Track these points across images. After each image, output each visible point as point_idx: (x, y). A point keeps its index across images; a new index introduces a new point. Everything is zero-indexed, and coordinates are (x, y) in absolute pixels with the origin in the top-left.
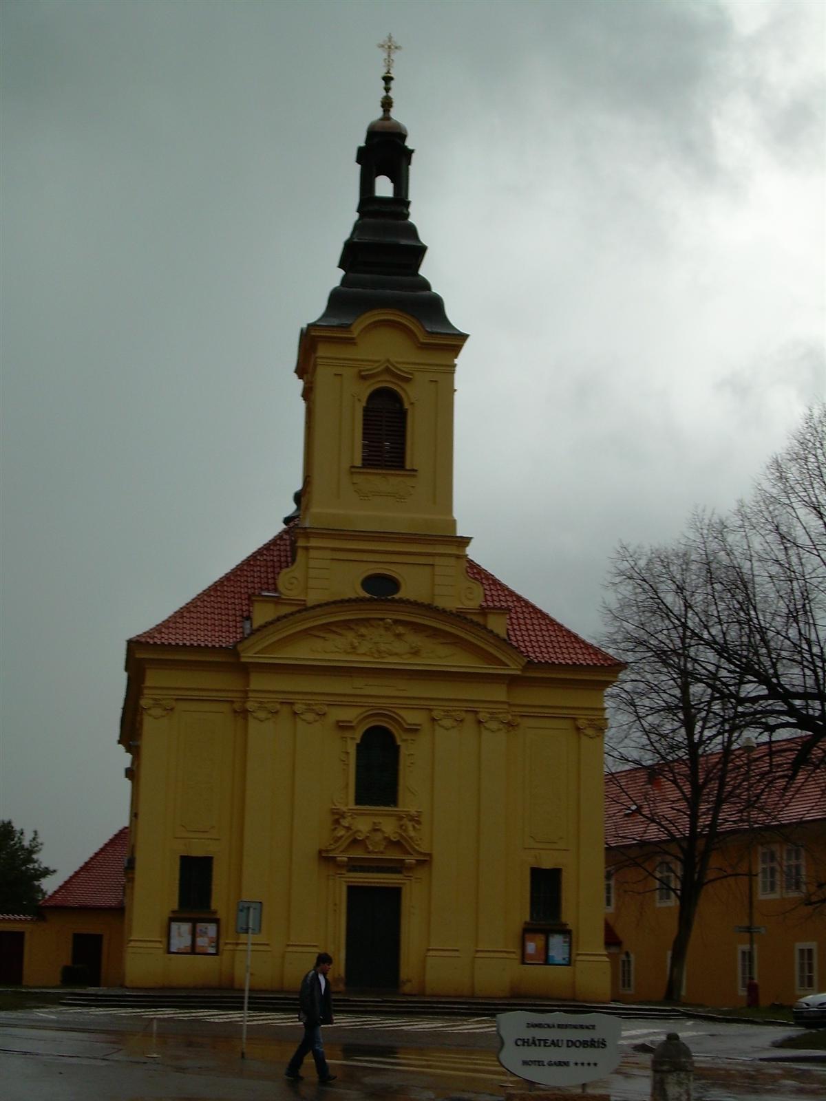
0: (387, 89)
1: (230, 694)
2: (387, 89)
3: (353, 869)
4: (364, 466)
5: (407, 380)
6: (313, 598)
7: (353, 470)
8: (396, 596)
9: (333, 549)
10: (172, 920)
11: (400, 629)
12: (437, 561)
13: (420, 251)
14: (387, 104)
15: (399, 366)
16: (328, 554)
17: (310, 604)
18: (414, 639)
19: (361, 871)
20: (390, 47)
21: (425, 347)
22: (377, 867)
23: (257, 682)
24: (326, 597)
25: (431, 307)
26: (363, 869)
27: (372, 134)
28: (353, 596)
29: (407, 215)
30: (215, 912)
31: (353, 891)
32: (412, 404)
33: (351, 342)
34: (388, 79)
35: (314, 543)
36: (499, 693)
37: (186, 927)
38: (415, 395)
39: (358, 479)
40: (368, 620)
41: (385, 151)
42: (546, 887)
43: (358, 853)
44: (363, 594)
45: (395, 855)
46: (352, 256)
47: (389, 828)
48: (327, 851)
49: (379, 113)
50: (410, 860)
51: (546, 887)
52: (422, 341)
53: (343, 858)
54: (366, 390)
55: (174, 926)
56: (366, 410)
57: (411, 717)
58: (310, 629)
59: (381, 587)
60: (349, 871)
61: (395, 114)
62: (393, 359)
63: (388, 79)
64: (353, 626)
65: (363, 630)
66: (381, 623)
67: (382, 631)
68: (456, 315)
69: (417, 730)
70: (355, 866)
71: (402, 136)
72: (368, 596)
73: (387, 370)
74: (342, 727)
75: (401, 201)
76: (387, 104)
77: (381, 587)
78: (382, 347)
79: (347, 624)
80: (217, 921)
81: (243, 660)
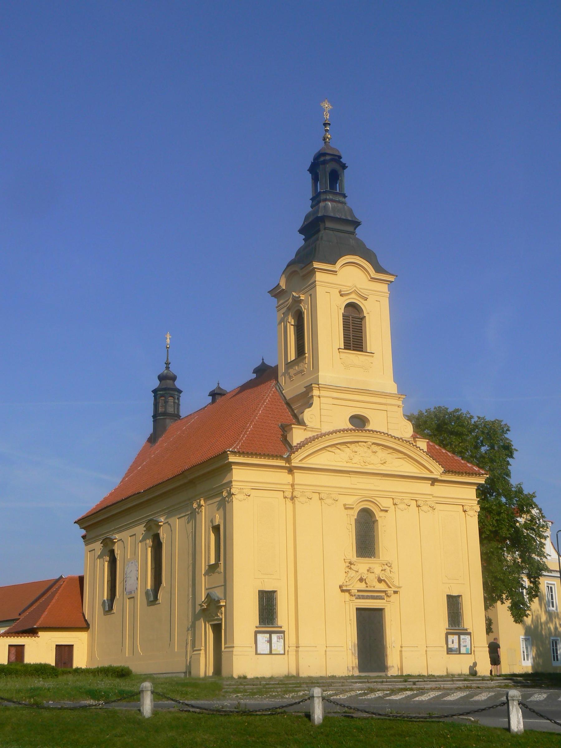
3: (359, 597)
4: (345, 349)
5: (366, 299)
7: (340, 350)
9: (333, 398)
11: (375, 448)
12: (389, 408)
15: (361, 290)
17: (323, 431)
18: (382, 454)
19: (363, 599)
21: (373, 279)
22: (371, 596)
23: (300, 477)
28: (346, 428)
30: (466, 630)
32: (368, 313)
35: (323, 393)
36: (425, 487)
37: (456, 638)
39: (343, 356)
40: (358, 442)
42: (454, 604)
44: (351, 427)
45: (382, 587)
50: (390, 591)
51: (454, 604)
52: (372, 276)
55: (259, 636)
57: (386, 503)
59: (359, 422)
60: (356, 598)
62: (358, 286)
64: (348, 445)
67: (366, 449)
69: (386, 511)
74: (347, 507)
77: (359, 422)
80: (469, 634)
81: (293, 465)
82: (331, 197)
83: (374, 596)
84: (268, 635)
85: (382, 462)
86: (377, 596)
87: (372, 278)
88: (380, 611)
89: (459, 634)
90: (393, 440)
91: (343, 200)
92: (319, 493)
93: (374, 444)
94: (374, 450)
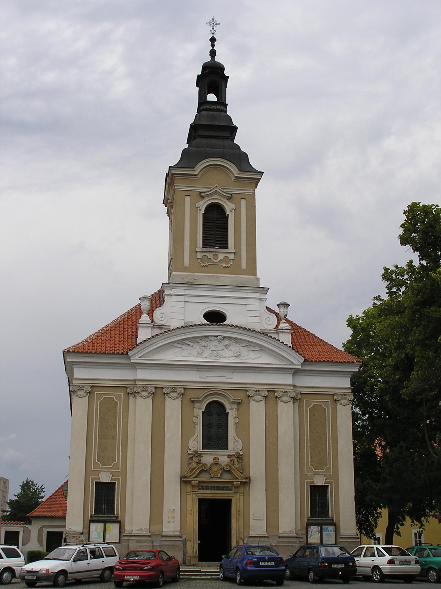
0: (213, 46)
1: (124, 383)
2: (213, 46)
6: (174, 324)
8: (224, 323)
10: (91, 521)
11: (227, 342)
13: (234, 129)
14: (213, 53)
16: (182, 298)
18: (235, 348)
19: (206, 489)
20: (213, 24)
22: (217, 487)
24: (181, 324)
25: (241, 159)
26: (207, 488)
27: (206, 67)
29: (226, 111)
31: (201, 502)
34: (213, 40)
40: (208, 337)
41: (212, 78)
43: (204, 477)
44: (205, 322)
45: (227, 478)
46: (195, 130)
47: (224, 460)
48: (185, 477)
49: (209, 59)
50: (237, 483)
53: (195, 482)
54: (203, 205)
55: (93, 526)
58: (173, 342)
61: (217, 59)
64: (198, 340)
65: (204, 344)
66: (215, 338)
67: (216, 343)
68: (255, 163)
70: (201, 486)
71: (222, 69)
72: (208, 323)
75: (222, 103)
76: (213, 53)
78: (215, 182)
79: (195, 340)
81: (132, 361)
82: (208, 107)
83: (220, 487)
84: (102, 524)
85: (236, 355)
86: (223, 487)
87: (236, 177)
88: (228, 502)
89: (320, 525)
90: (245, 332)
91: (222, 108)
93: (224, 337)
94: (226, 344)
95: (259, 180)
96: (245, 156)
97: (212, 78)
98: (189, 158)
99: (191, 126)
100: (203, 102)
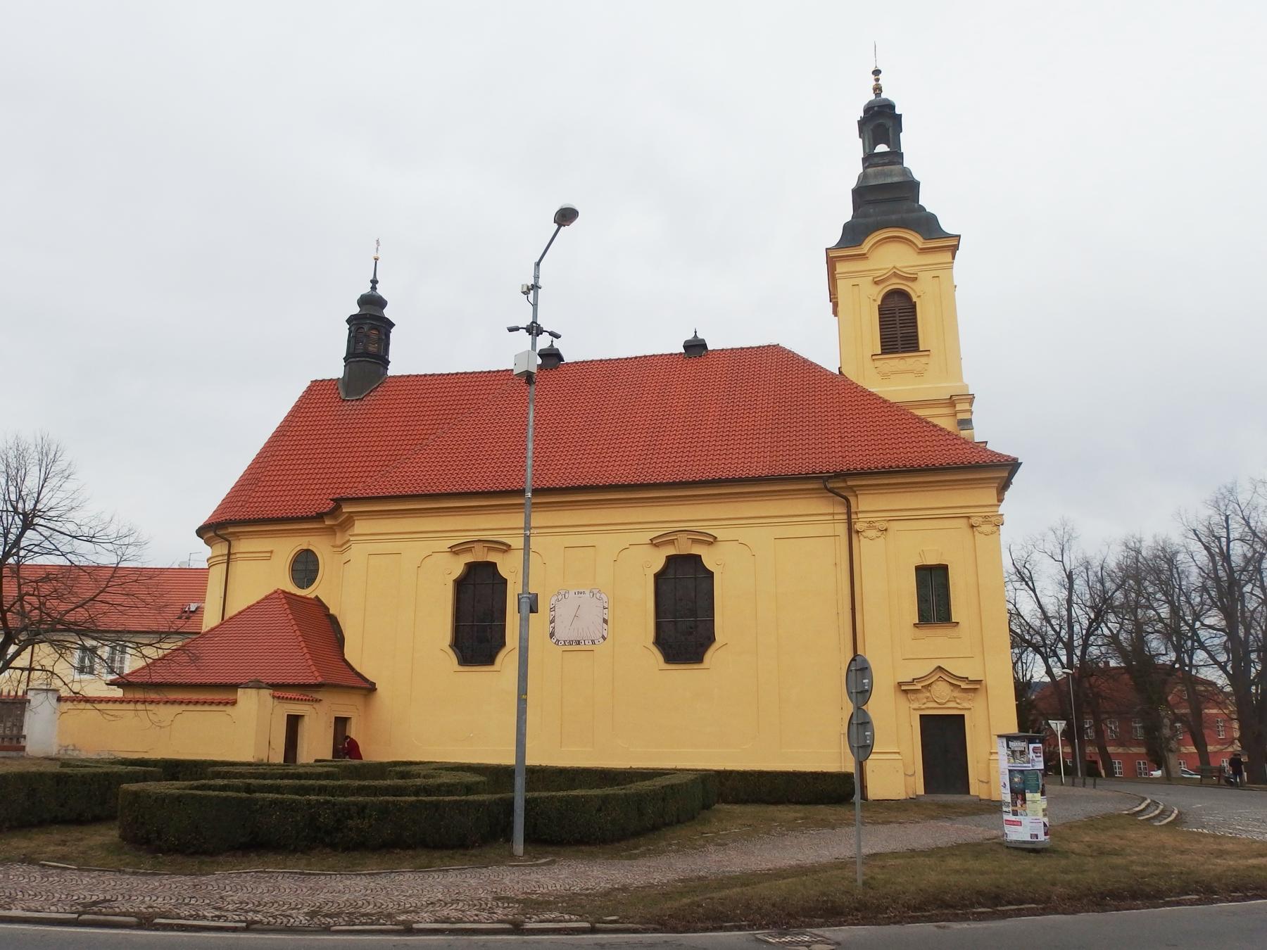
0: (877, 80)
2: (877, 80)
14: (878, 90)
21: (923, 251)
25: (927, 226)
27: (869, 109)
33: (863, 257)
34: (877, 72)
38: (922, 294)
39: (878, 363)
41: (880, 122)
46: (862, 195)
49: (873, 97)
54: (878, 293)
56: (880, 308)
61: (883, 96)
62: (898, 265)
63: (877, 72)
68: (947, 225)
73: (895, 275)
75: (896, 156)
76: (878, 90)
92: (969, 517)
95: (956, 247)
96: (932, 219)
97: (880, 122)
98: (853, 234)
99: (855, 192)
100: (870, 159)
